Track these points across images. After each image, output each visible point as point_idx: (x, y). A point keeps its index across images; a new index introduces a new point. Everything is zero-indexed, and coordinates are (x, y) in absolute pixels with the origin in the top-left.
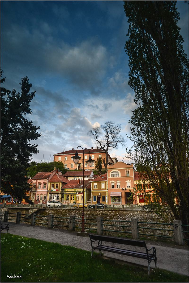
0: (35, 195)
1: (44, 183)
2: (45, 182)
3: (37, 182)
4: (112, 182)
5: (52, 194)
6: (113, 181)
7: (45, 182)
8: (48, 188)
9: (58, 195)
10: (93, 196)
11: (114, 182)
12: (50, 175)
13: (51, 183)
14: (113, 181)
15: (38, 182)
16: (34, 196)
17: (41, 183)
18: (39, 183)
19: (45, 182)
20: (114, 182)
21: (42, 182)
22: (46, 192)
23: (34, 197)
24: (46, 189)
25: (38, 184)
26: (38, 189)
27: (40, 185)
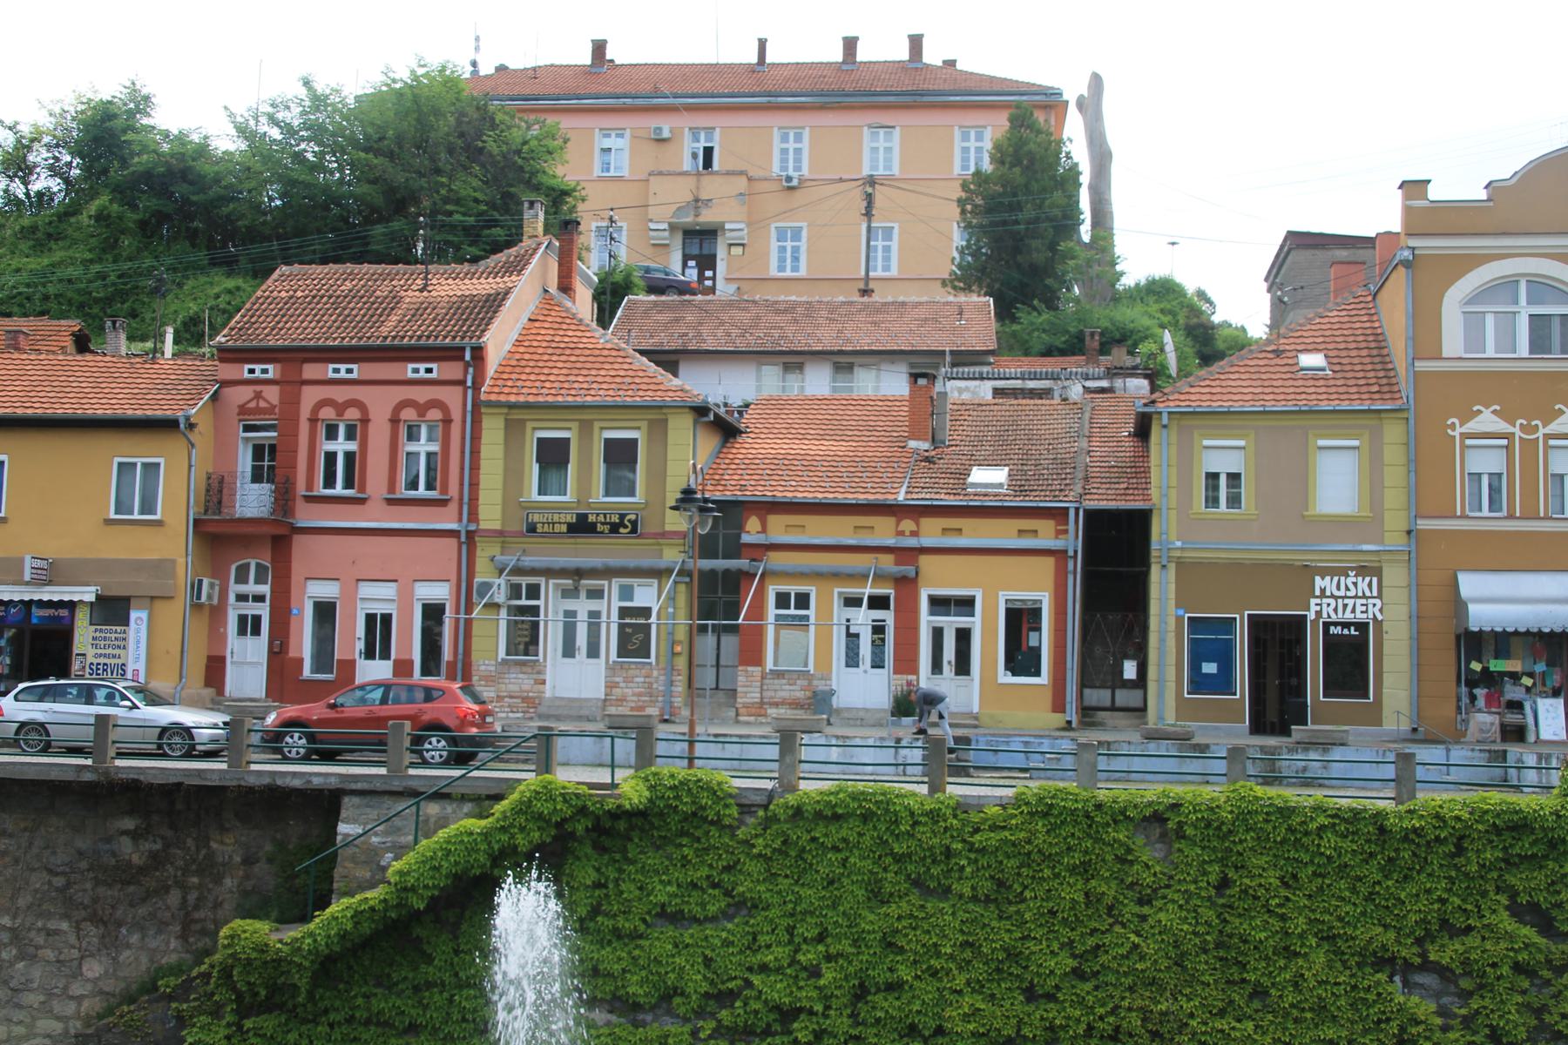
0: (265, 589)
1: (409, 414)
2: (435, 404)
3: (291, 403)
4: (1473, 426)
5: (549, 573)
6: (1487, 420)
7: (422, 394)
8: (474, 485)
9: (646, 595)
10: (1179, 619)
11: (1503, 426)
12: (493, 304)
13: (517, 415)
14: (1487, 420)
15: (310, 396)
16: (259, 598)
17: (365, 421)
18: (327, 413)
19: (422, 394)
20: (1503, 426)
21: (380, 403)
22: (453, 542)
23: (251, 609)
24: (442, 503)
25: (313, 421)
26: (309, 499)
27: (341, 446)
